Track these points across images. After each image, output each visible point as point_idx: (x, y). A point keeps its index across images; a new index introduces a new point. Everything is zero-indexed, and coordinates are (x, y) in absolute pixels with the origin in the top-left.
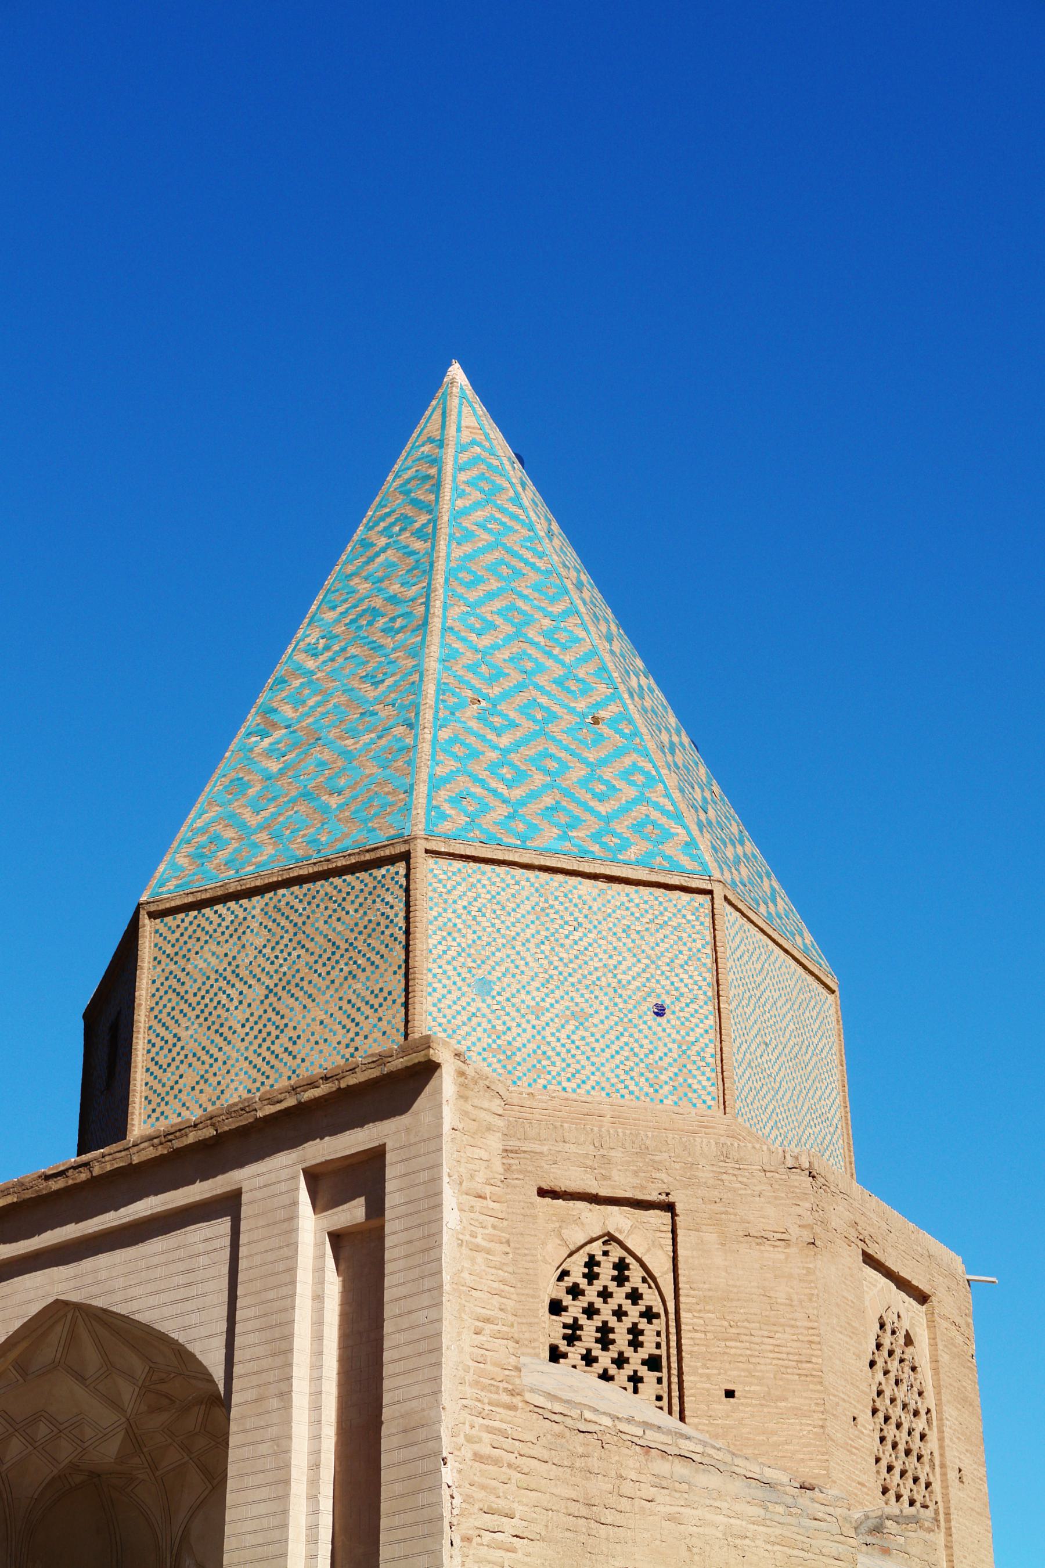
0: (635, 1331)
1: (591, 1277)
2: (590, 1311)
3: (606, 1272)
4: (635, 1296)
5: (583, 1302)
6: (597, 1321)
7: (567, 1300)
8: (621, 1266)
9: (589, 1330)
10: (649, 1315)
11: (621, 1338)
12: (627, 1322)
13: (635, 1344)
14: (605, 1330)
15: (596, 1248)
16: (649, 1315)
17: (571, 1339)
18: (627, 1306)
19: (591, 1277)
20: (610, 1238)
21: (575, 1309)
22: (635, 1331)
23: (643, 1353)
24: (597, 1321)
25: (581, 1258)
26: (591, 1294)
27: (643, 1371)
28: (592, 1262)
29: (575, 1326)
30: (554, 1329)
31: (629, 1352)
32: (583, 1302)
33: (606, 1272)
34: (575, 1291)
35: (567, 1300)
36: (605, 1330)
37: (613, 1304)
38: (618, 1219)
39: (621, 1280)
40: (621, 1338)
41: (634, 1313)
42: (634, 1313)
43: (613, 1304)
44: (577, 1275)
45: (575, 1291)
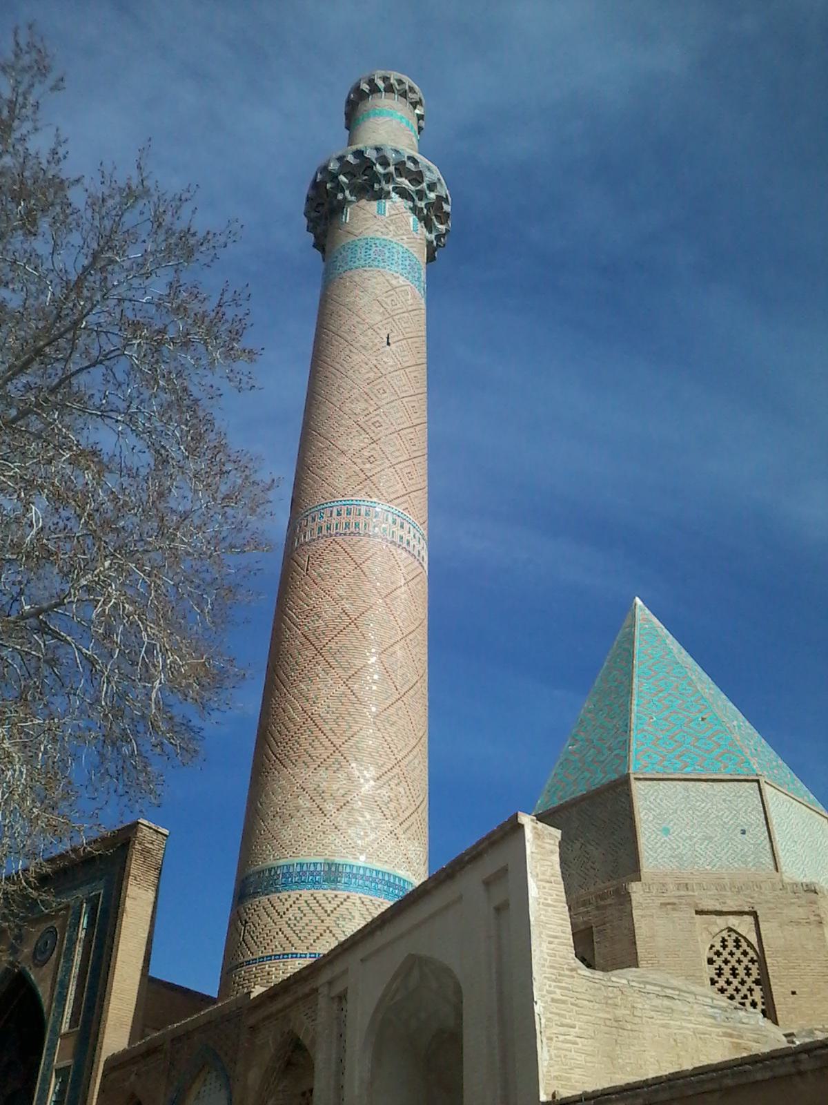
1: (724, 947)
2: (726, 962)
3: (731, 944)
4: (745, 953)
6: (730, 966)
7: (715, 958)
8: (737, 941)
9: (727, 970)
12: (743, 965)
13: (748, 974)
14: (733, 969)
15: (725, 934)
16: (752, 961)
17: (719, 975)
18: (742, 958)
19: (724, 947)
20: (730, 930)
21: (719, 962)
23: (752, 978)
24: (730, 966)
26: (725, 954)
27: (754, 986)
28: (724, 940)
29: (720, 969)
30: (710, 971)
31: (746, 978)
32: (722, 958)
33: (731, 944)
34: (718, 954)
35: (715, 958)
36: (733, 969)
37: (736, 957)
38: (733, 921)
39: (738, 947)
41: (745, 961)
43: (736, 957)
44: (718, 947)
45: (718, 954)
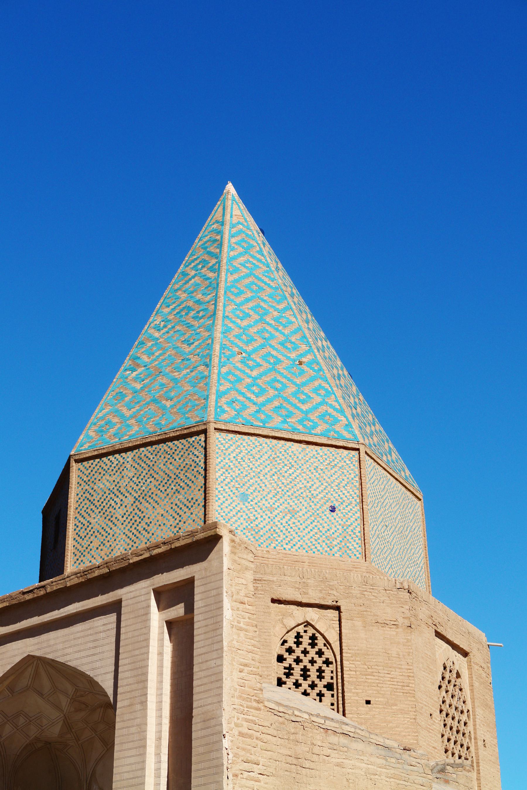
0: (320, 671)
1: (298, 644)
2: (298, 661)
3: (306, 641)
4: (320, 653)
5: (294, 656)
6: (301, 666)
7: (286, 655)
9: (297, 670)
10: (327, 662)
11: (313, 674)
12: (316, 666)
13: (320, 677)
14: (305, 670)
15: (301, 629)
16: (327, 662)
18: (316, 658)
19: (298, 644)
21: (290, 659)
22: (320, 671)
24: (301, 666)
25: (293, 634)
26: (298, 652)
28: (298, 636)
29: (290, 668)
32: (294, 656)
33: (306, 641)
34: (290, 651)
35: (286, 655)
36: (305, 670)
37: (309, 657)
39: (313, 645)
40: (313, 674)
41: (320, 661)
42: (320, 661)
43: (309, 657)
44: (291, 643)
45: (290, 651)
